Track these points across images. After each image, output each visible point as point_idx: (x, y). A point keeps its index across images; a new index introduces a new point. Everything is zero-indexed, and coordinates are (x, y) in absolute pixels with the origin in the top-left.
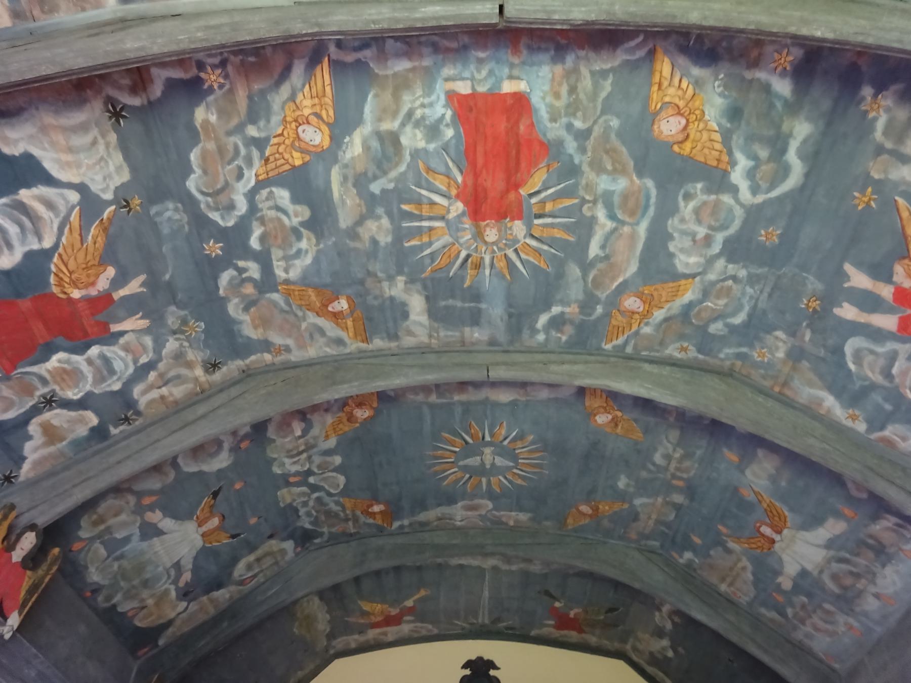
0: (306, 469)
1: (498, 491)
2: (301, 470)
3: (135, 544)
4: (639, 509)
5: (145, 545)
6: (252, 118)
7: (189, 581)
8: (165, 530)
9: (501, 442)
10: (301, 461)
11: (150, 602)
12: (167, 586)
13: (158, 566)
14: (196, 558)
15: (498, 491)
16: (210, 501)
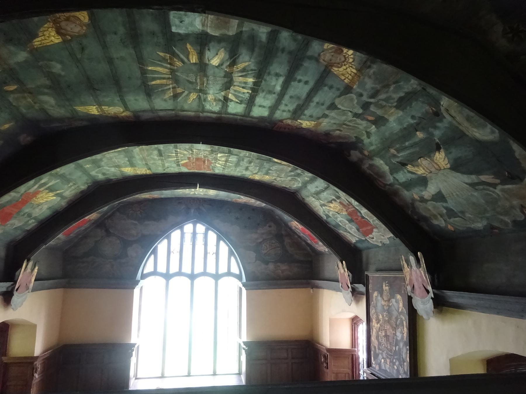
0: (355, 118)
1: (189, 46)
2: (359, 119)
3: (451, 204)
4: (12, 48)
5: (449, 201)
6: (273, 182)
7: (493, 176)
8: (438, 191)
9: (190, 93)
10: (353, 123)
11: (516, 202)
12: (497, 191)
13: (472, 195)
14: (463, 173)
15: (189, 46)
16: (410, 167)
